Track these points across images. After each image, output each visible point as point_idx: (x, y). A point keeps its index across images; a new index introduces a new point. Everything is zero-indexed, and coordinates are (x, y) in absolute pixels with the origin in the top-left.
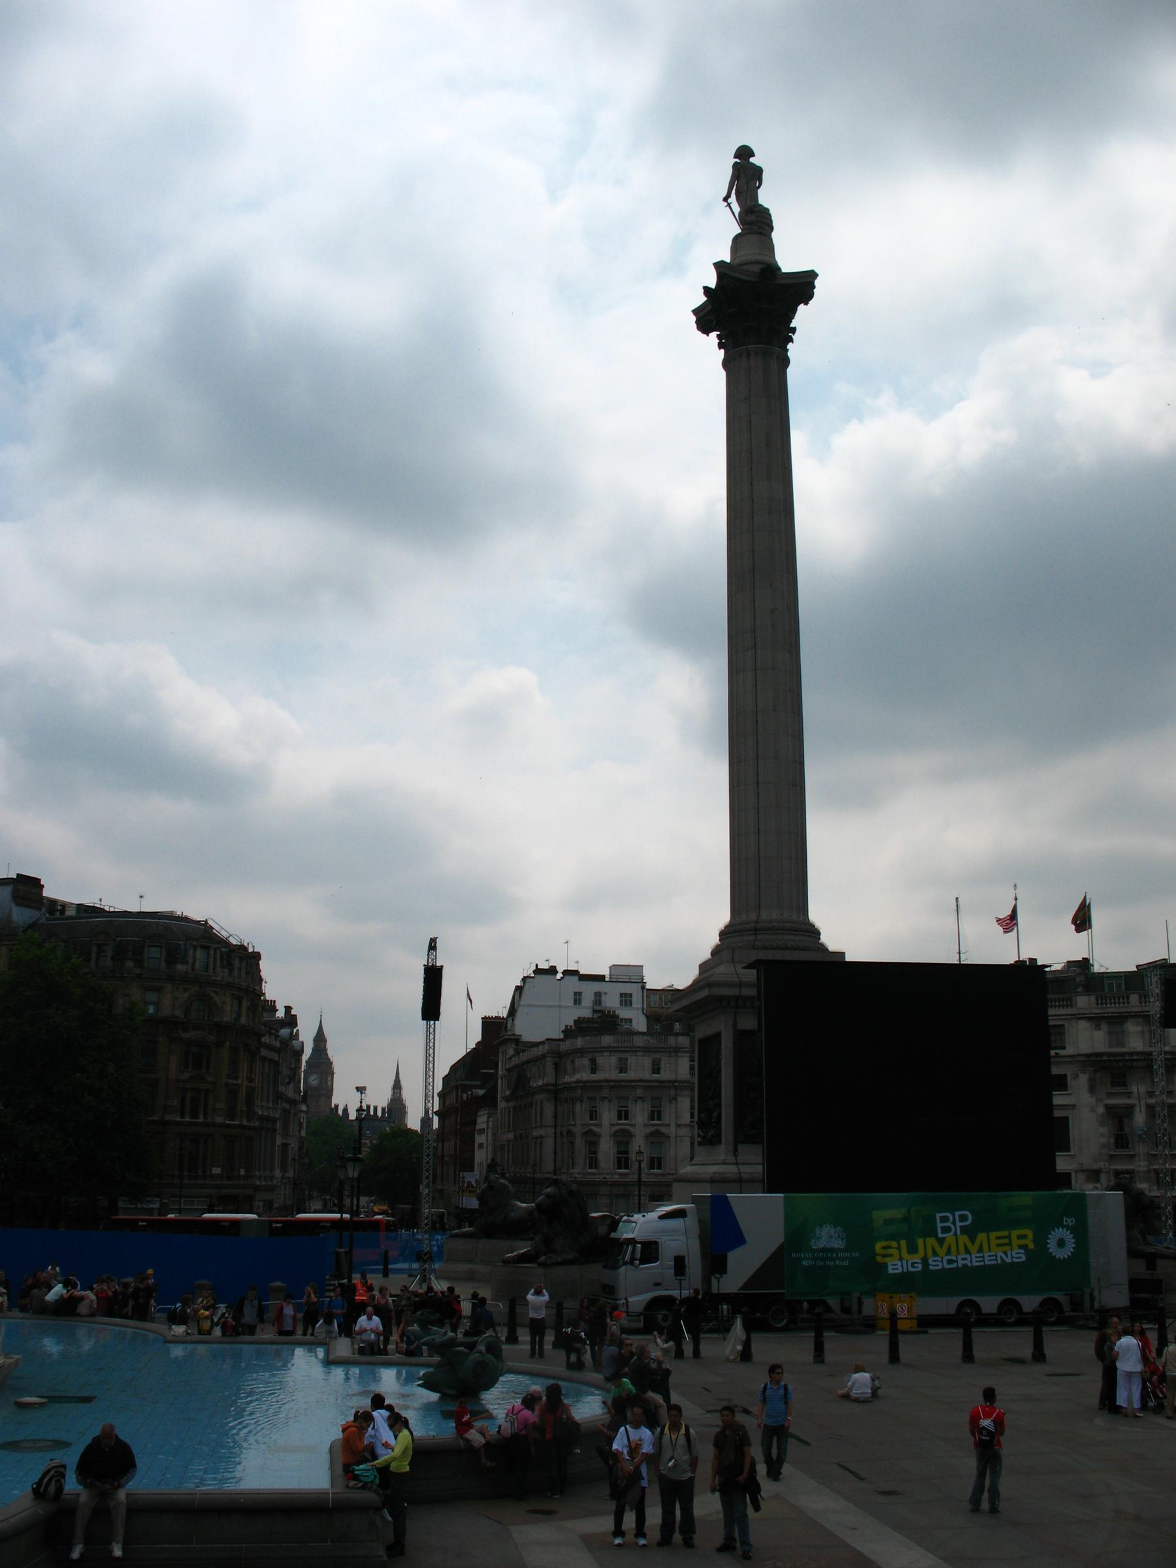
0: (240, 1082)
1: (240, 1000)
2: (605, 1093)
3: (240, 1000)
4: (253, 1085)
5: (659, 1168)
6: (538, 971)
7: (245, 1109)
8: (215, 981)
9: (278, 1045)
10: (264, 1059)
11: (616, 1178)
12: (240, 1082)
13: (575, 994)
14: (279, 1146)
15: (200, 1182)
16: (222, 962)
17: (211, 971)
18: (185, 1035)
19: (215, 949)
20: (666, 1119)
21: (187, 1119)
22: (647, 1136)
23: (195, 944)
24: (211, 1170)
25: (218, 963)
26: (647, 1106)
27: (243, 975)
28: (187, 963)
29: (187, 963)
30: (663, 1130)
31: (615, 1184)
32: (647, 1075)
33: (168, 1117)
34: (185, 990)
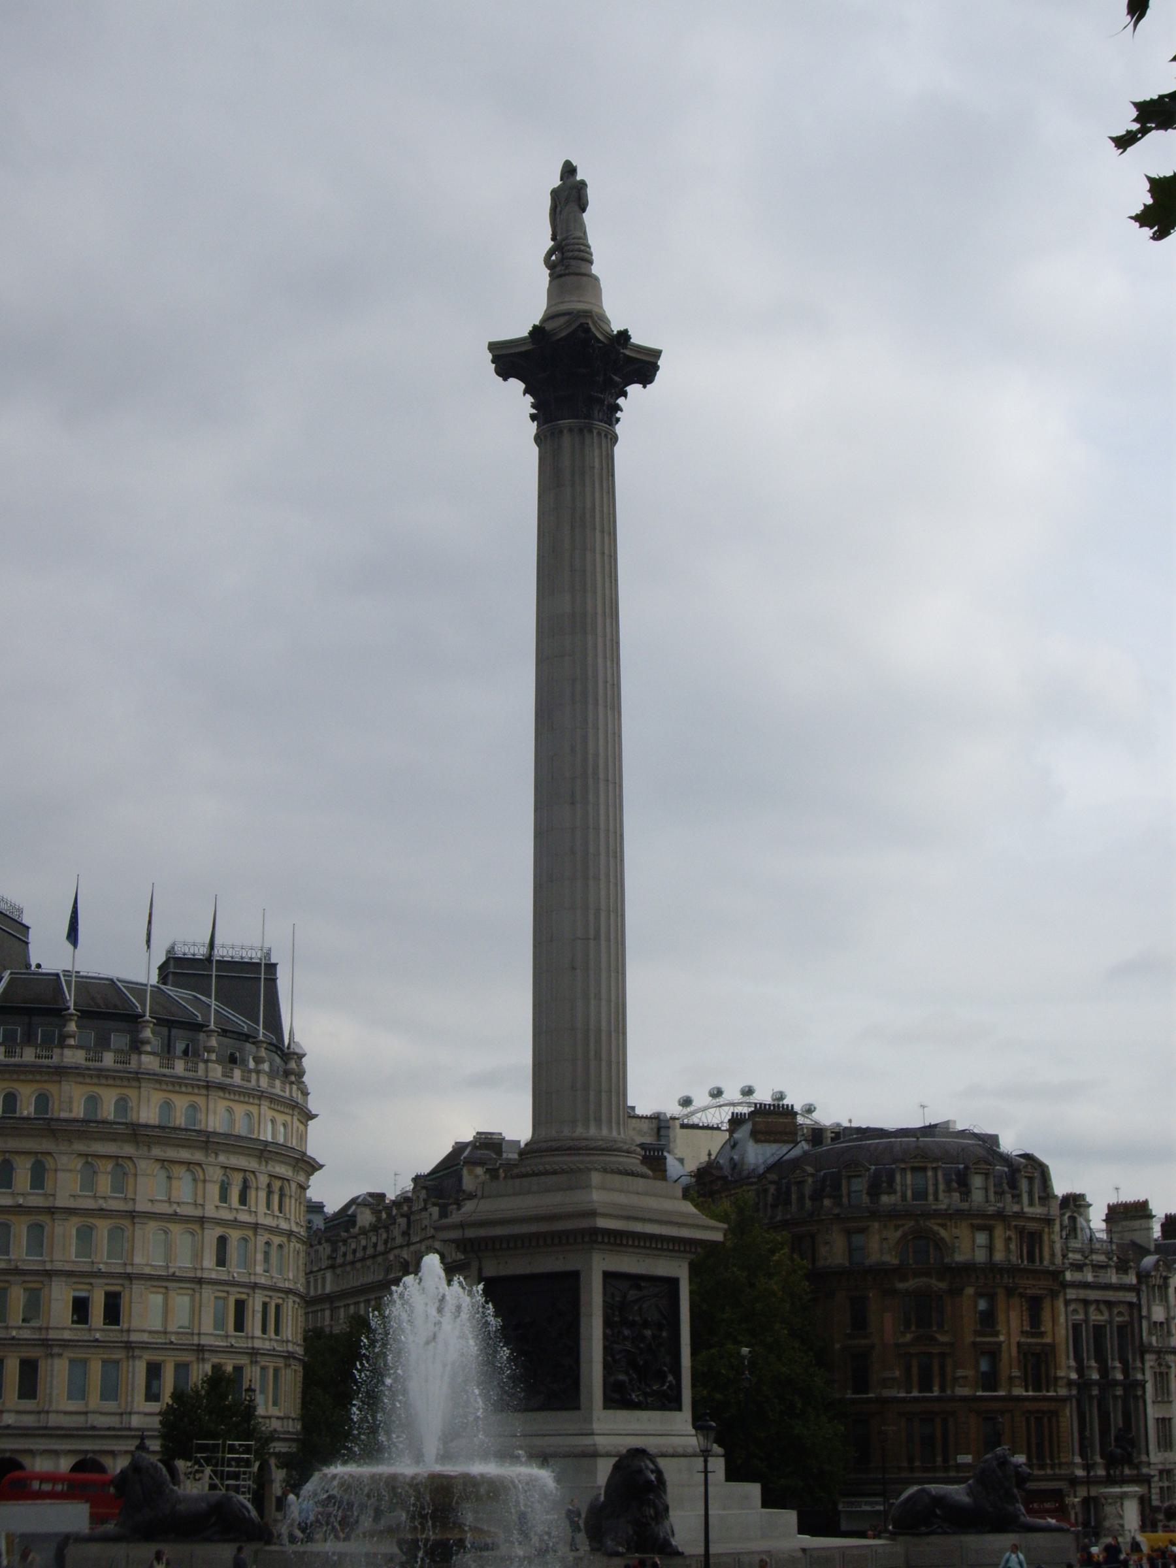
0: (1002, 1338)
1: (990, 1230)
3: (990, 1230)
7: (1016, 1373)
8: (935, 1210)
9: (1132, 1279)
10: (1086, 1303)
12: (1002, 1338)
15: (940, 1475)
16: (948, 1183)
17: (931, 1198)
18: (901, 1286)
19: (935, 1169)
21: (915, 1394)
23: (903, 1166)
24: (956, 1459)
25: (941, 1187)
27: (992, 1198)
28: (895, 1192)
29: (895, 1192)
33: (887, 1393)
34: (897, 1227)
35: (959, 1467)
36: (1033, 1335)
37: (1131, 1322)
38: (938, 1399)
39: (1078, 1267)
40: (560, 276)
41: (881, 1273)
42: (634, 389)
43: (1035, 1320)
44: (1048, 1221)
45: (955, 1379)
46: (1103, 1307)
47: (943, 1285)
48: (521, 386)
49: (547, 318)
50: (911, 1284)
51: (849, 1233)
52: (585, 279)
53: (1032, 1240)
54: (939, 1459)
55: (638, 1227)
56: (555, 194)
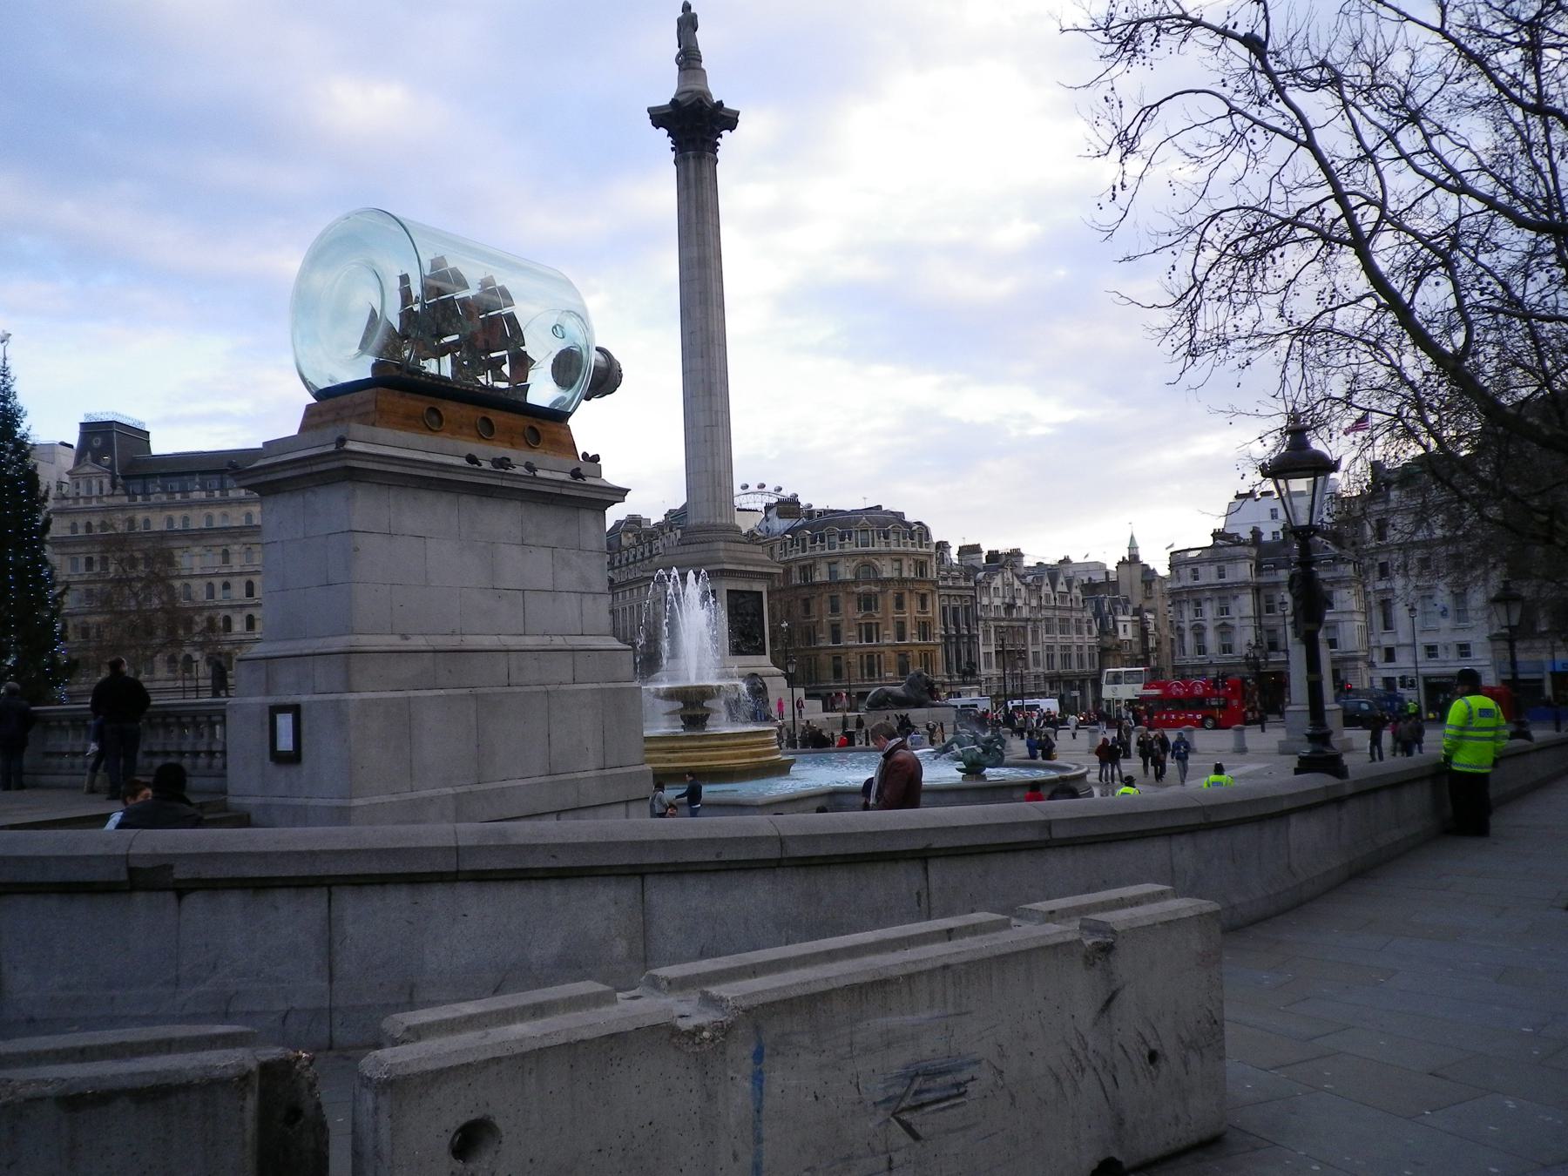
2: (1185, 597)
3: (900, 561)
4: (930, 615)
5: (1230, 652)
6: (1238, 496)
11: (1196, 662)
13: (1272, 510)
14: (988, 654)
20: (1233, 612)
21: (864, 643)
22: (1217, 628)
26: (1216, 604)
30: (1229, 622)
31: (1194, 667)
32: (1214, 580)
34: (854, 561)
35: (886, 679)
36: (923, 613)
37: (972, 606)
38: (875, 646)
39: (945, 579)
40: (685, 69)
41: (845, 583)
42: (725, 133)
43: (923, 605)
44: (930, 555)
45: (884, 635)
46: (958, 598)
47: (878, 589)
48: (666, 132)
49: (678, 94)
50: (862, 589)
51: (829, 564)
52: (698, 71)
53: (921, 566)
54: (877, 676)
55: (743, 568)
56: (679, 21)
